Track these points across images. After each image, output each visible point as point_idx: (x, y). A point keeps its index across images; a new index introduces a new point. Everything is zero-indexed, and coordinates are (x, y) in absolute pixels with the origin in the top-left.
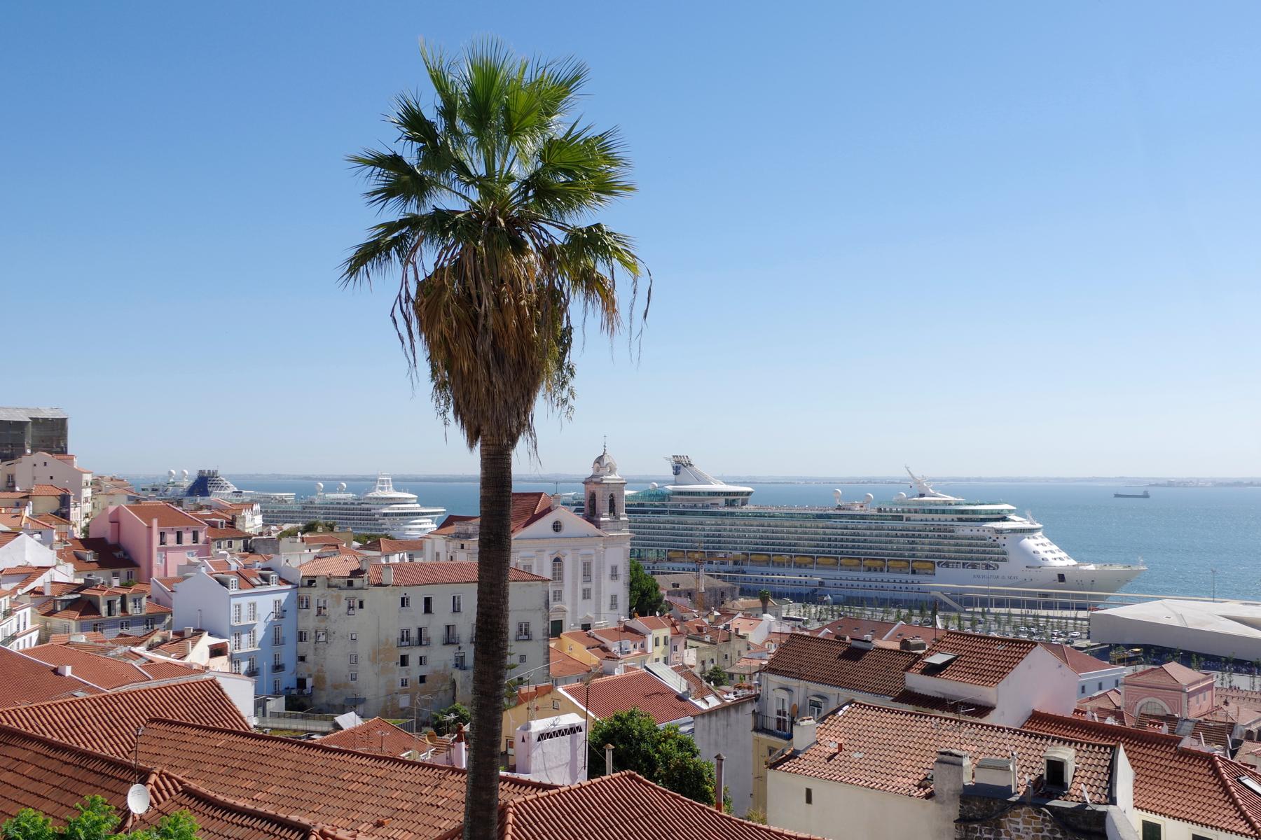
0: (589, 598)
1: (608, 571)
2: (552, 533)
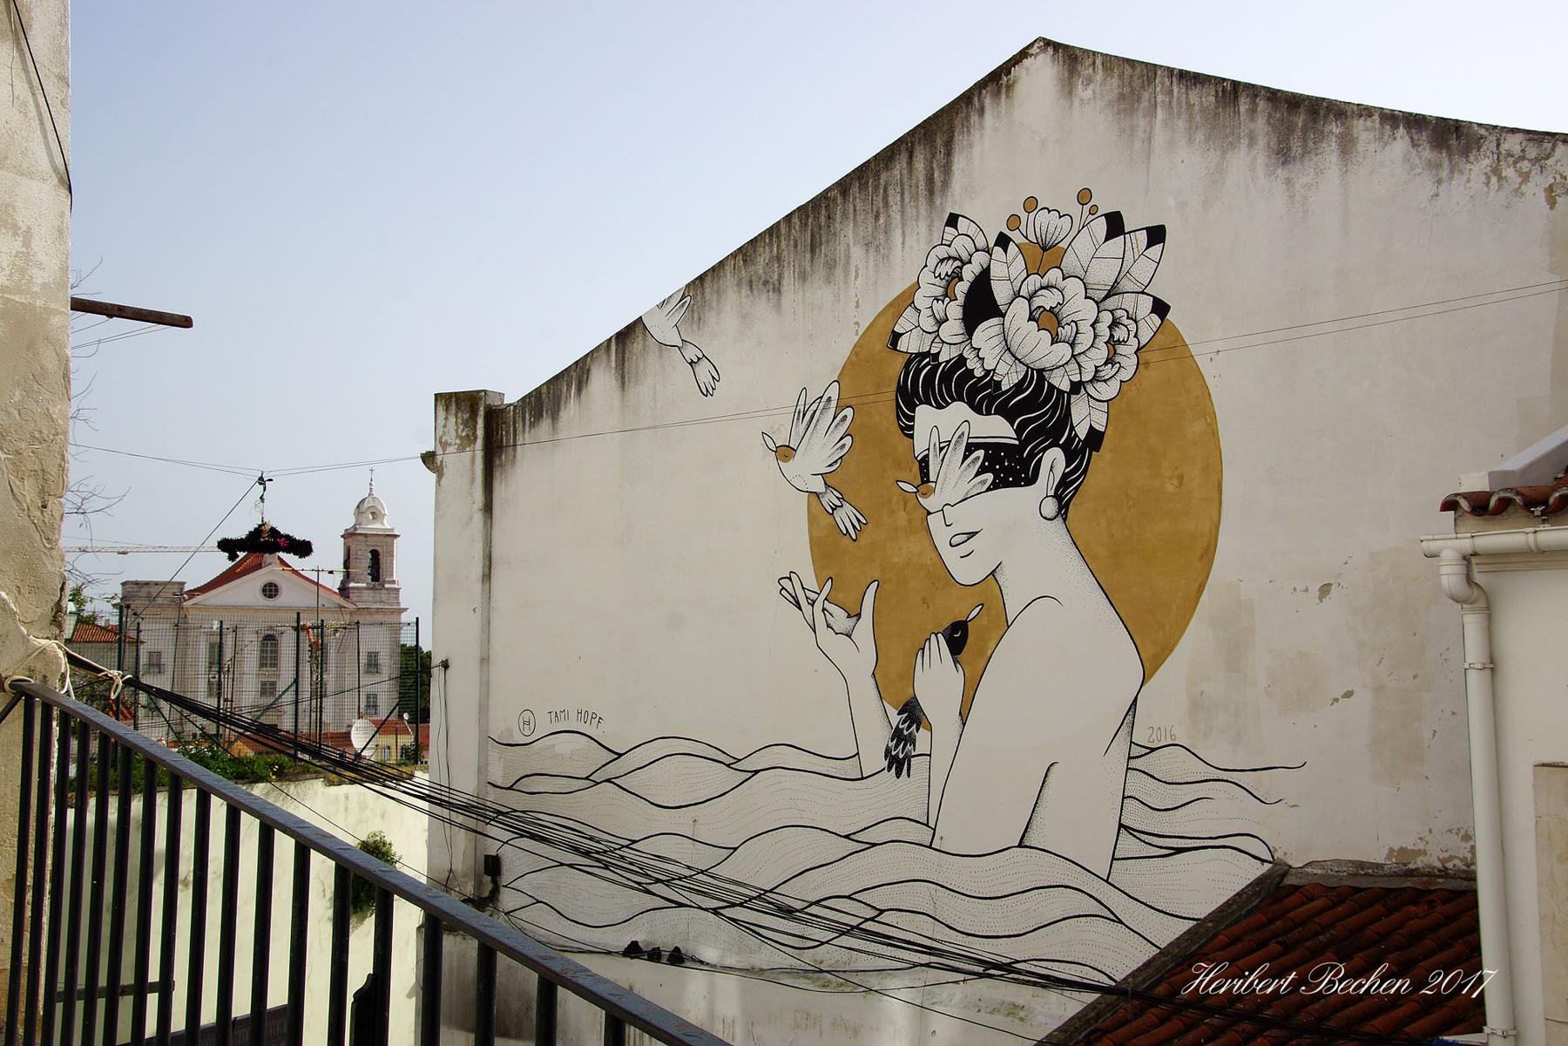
2: (262, 601)
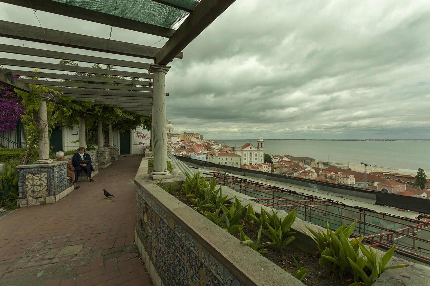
0: (256, 159)
1: (260, 155)
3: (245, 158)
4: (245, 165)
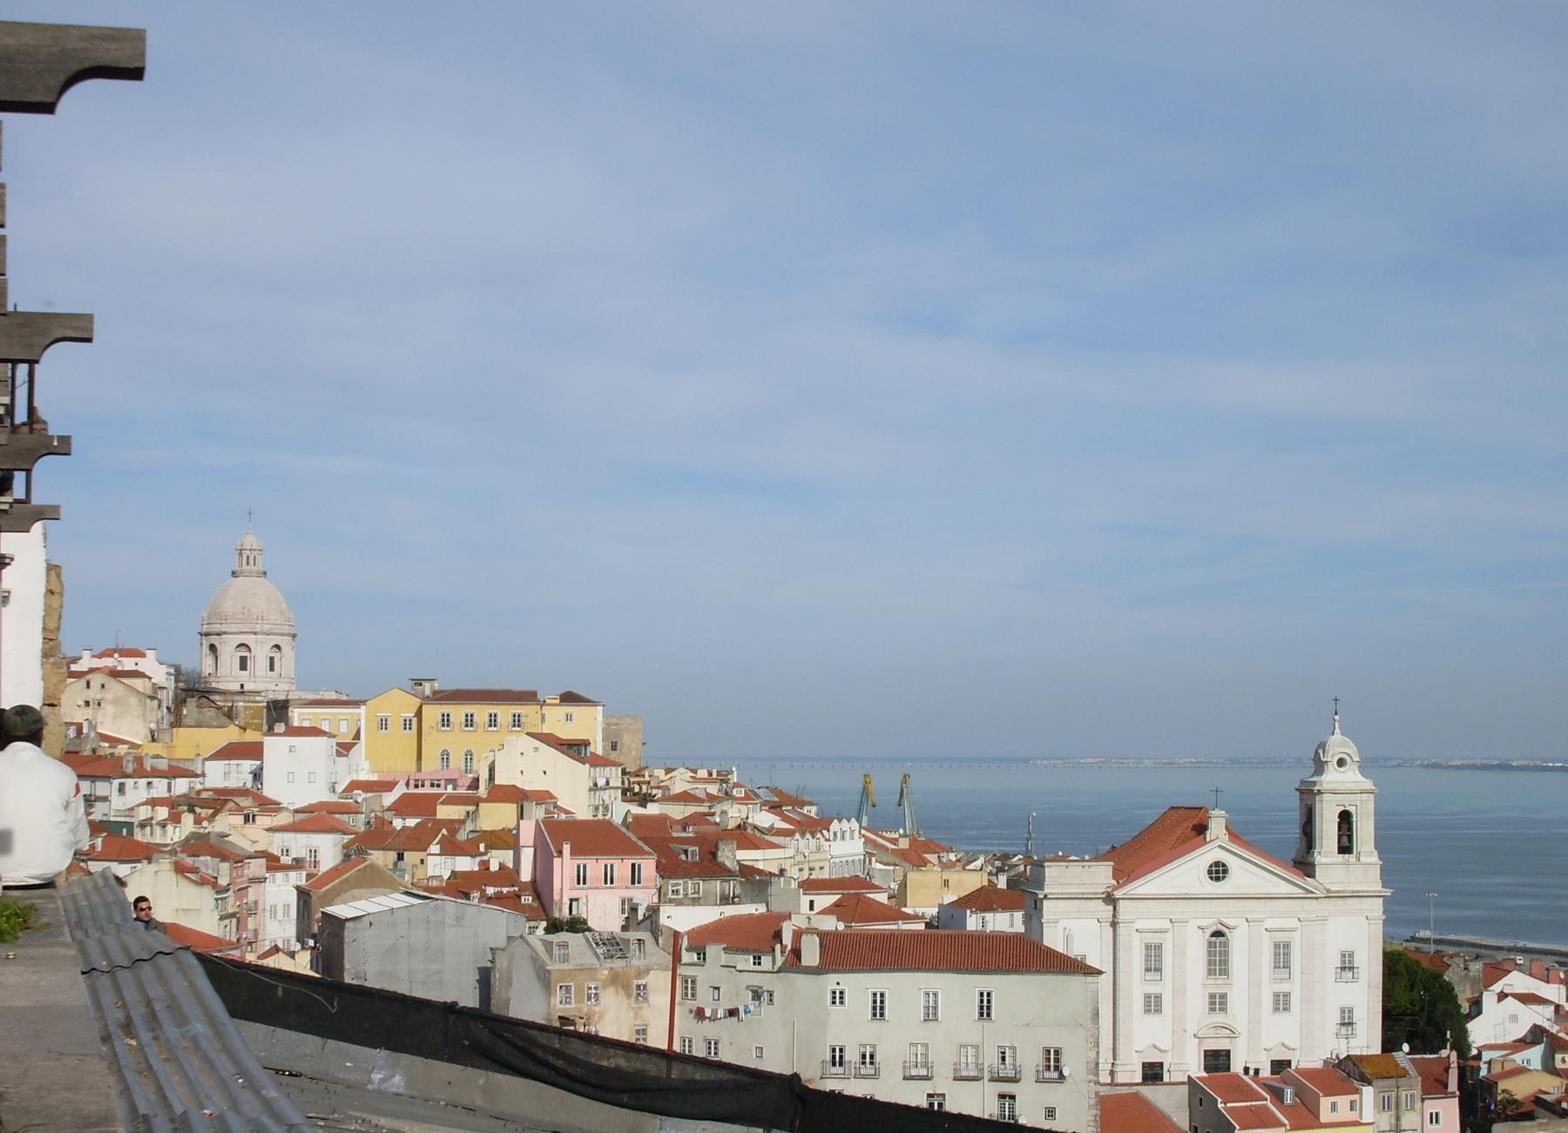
3: (1153, 989)
4: (1153, 1073)
